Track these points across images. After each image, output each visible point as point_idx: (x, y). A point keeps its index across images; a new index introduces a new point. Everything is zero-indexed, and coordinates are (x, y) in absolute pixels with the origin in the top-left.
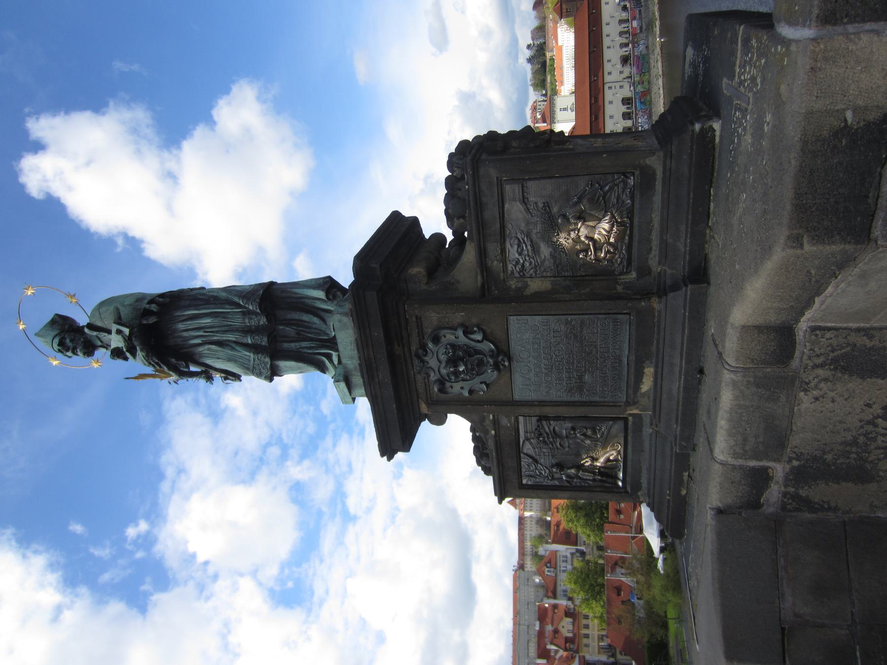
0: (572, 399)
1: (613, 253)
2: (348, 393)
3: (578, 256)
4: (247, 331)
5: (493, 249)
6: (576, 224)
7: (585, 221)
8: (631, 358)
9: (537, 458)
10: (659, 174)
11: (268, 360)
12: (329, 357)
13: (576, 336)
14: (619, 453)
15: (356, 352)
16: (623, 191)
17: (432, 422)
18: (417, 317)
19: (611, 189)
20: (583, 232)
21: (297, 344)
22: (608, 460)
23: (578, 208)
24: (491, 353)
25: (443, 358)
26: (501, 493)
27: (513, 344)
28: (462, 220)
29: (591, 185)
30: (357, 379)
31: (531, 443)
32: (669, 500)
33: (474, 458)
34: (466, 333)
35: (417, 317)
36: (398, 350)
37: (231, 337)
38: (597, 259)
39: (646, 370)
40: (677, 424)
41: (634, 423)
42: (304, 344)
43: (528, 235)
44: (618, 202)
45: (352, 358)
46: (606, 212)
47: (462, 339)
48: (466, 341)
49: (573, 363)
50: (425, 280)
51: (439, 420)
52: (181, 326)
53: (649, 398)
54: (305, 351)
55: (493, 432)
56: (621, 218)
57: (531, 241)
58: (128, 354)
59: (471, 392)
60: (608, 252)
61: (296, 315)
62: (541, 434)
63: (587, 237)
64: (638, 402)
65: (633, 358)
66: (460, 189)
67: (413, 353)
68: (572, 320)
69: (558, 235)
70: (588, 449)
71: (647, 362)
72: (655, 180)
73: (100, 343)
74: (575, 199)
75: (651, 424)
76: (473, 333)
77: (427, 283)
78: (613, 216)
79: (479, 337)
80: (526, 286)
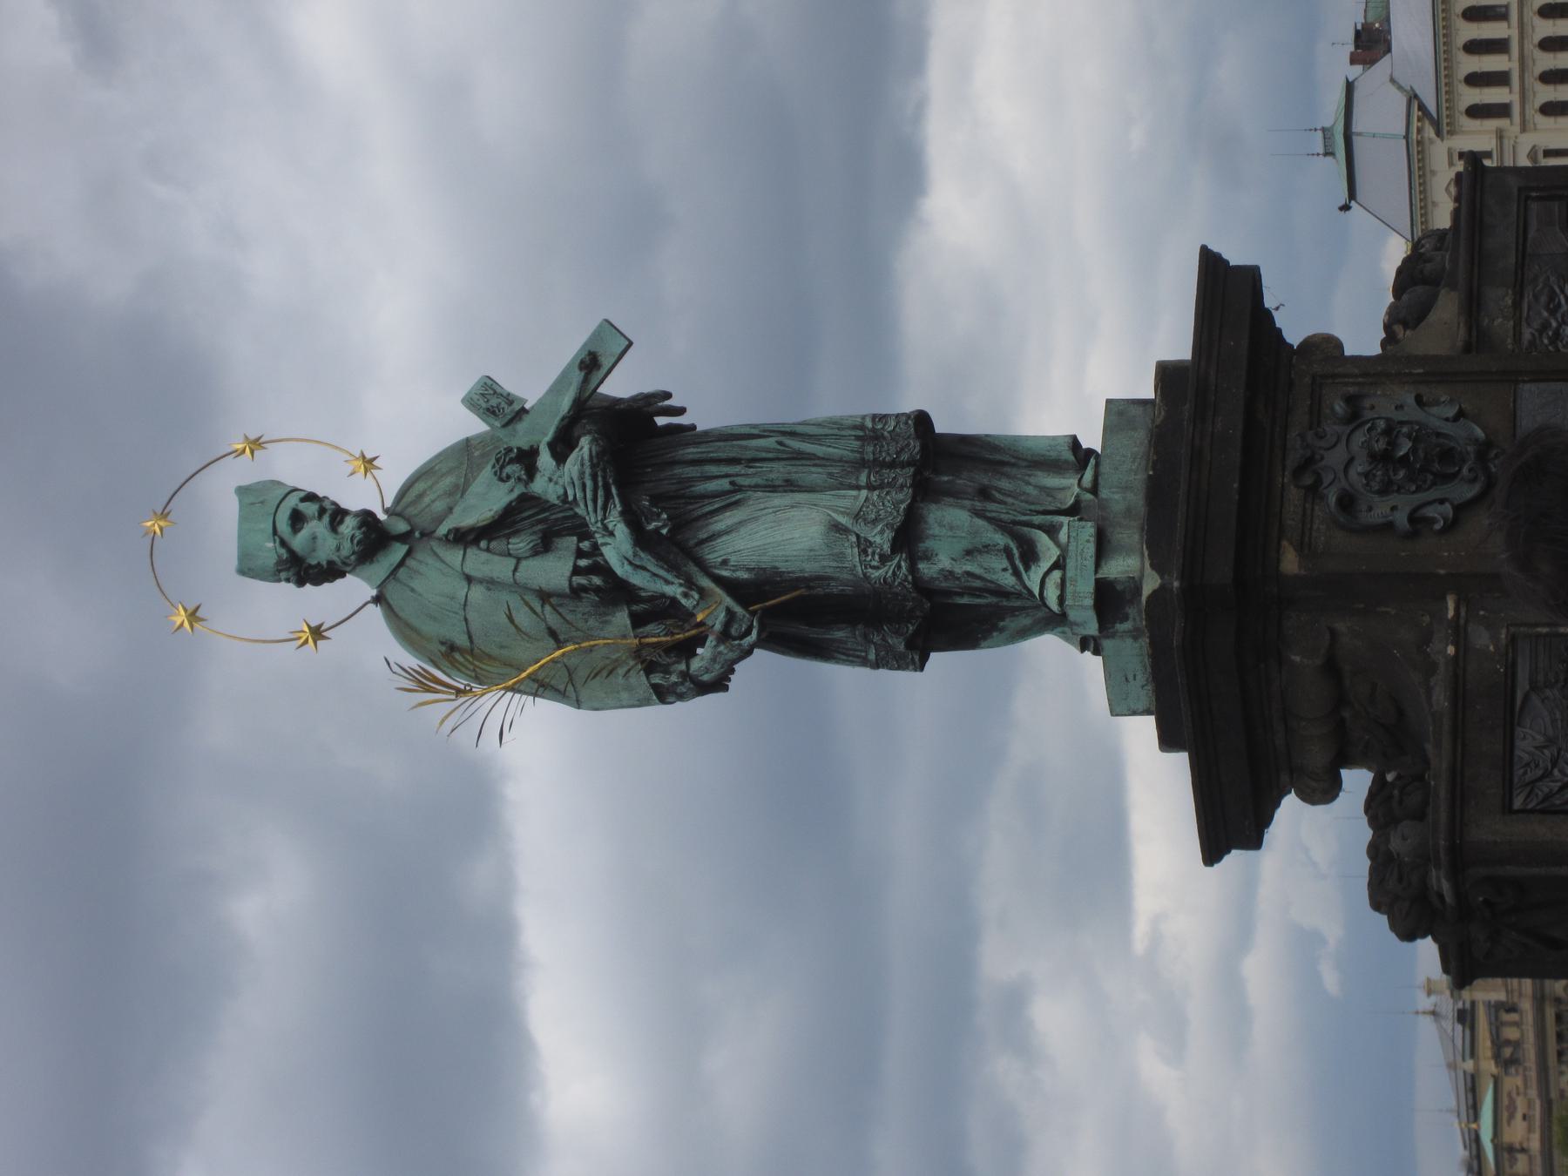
2: (1091, 563)
4: (861, 464)
5: (1499, 298)
11: (904, 497)
12: (1052, 531)
15: (1141, 476)
30: (1129, 535)
34: (1419, 400)
37: (815, 475)
45: (1126, 488)
47: (1412, 412)
52: (691, 452)
55: (1451, 650)
58: (545, 460)
59: (1412, 519)
61: (984, 479)
73: (401, 527)
79: (1451, 412)
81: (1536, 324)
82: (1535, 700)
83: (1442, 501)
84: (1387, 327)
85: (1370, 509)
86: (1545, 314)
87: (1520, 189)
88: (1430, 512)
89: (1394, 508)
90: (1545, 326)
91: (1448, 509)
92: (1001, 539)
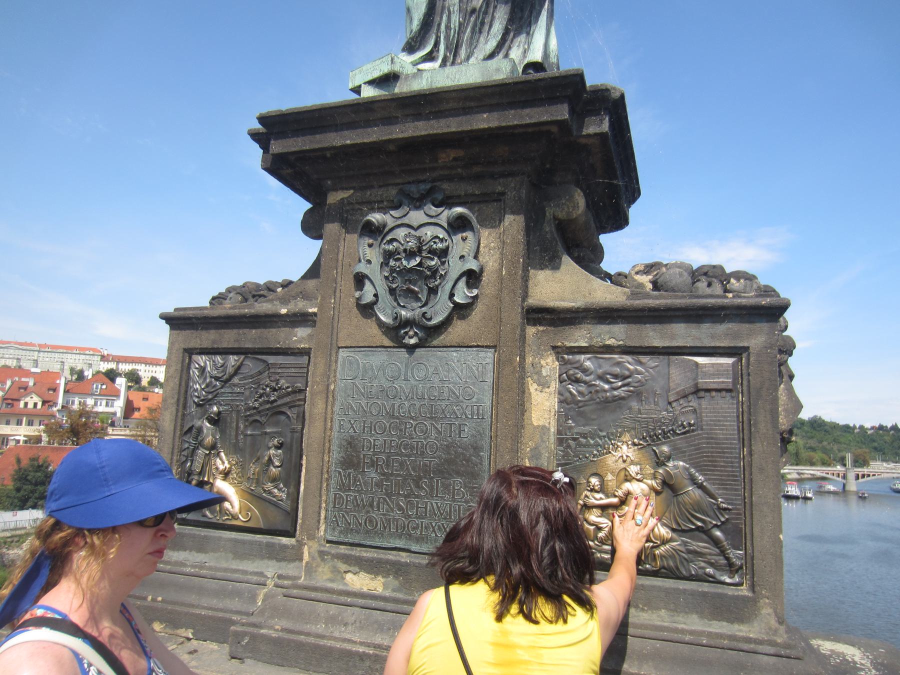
0: (335, 448)
1: (596, 538)
2: (370, 78)
3: (595, 474)
5: (613, 334)
6: (654, 477)
7: (658, 493)
8: (404, 554)
9: (236, 380)
10: (741, 630)
13: (449, 462)
14: (235, 517)
16: (712, 565)
17: (308, 214)
18: (503, 194)
19: (716, 542)
20: (636, 488)
21: (457, 8)
22: (221, 499)
23: (687, 482)
24: (428, 316)
25: (429, 232)
26: (178, 321)
27: (440, 353)
28: (650, 286)
29: (725, 509)
31: (260, 373)
32: (145, 599)
33: (239, 283)
35: (503, 194)
36: (447, 156)
38: (587, 507)
39: (381, 579)
40: (283, 630)
41: (285, 547)
42: (456, 19)
43: (637, 395)
44: (689, 552)
46: (673, 530)
47: (455, 267)
48: (454, 274)
49: (402, 455)
50: (562, 215)
51: (312, 226)
53: (332, 581)
54: (445, 18)
55: (284, 311)
56: (662, 556)
57: (623, 398)
60: (599, 529)
62: (274, 390)
63: (628, 494)
64: (323, 560)
65: (404, 557)
66: (709, 285)
67: (438, 184)
68: (481, 458)
69: (634, 444)
70: (243, 467)
71: (396, 583)
72: (731, 621)
74: (701, 478)
75: (280, 577)
76: (469, 286)
77: (555, 218)
78: (664, 542)
80: (543, 384)
81: (588, 364)
82: (261, 367)
83: (376, 295)
84: (666, 265)
85: (370, 246)
86: (600, 371)
87: (746, 349)
88: (368, 286)
89: (369, 262)
90: (585, 371)
91: (368, 298)
92: (416, 25)
